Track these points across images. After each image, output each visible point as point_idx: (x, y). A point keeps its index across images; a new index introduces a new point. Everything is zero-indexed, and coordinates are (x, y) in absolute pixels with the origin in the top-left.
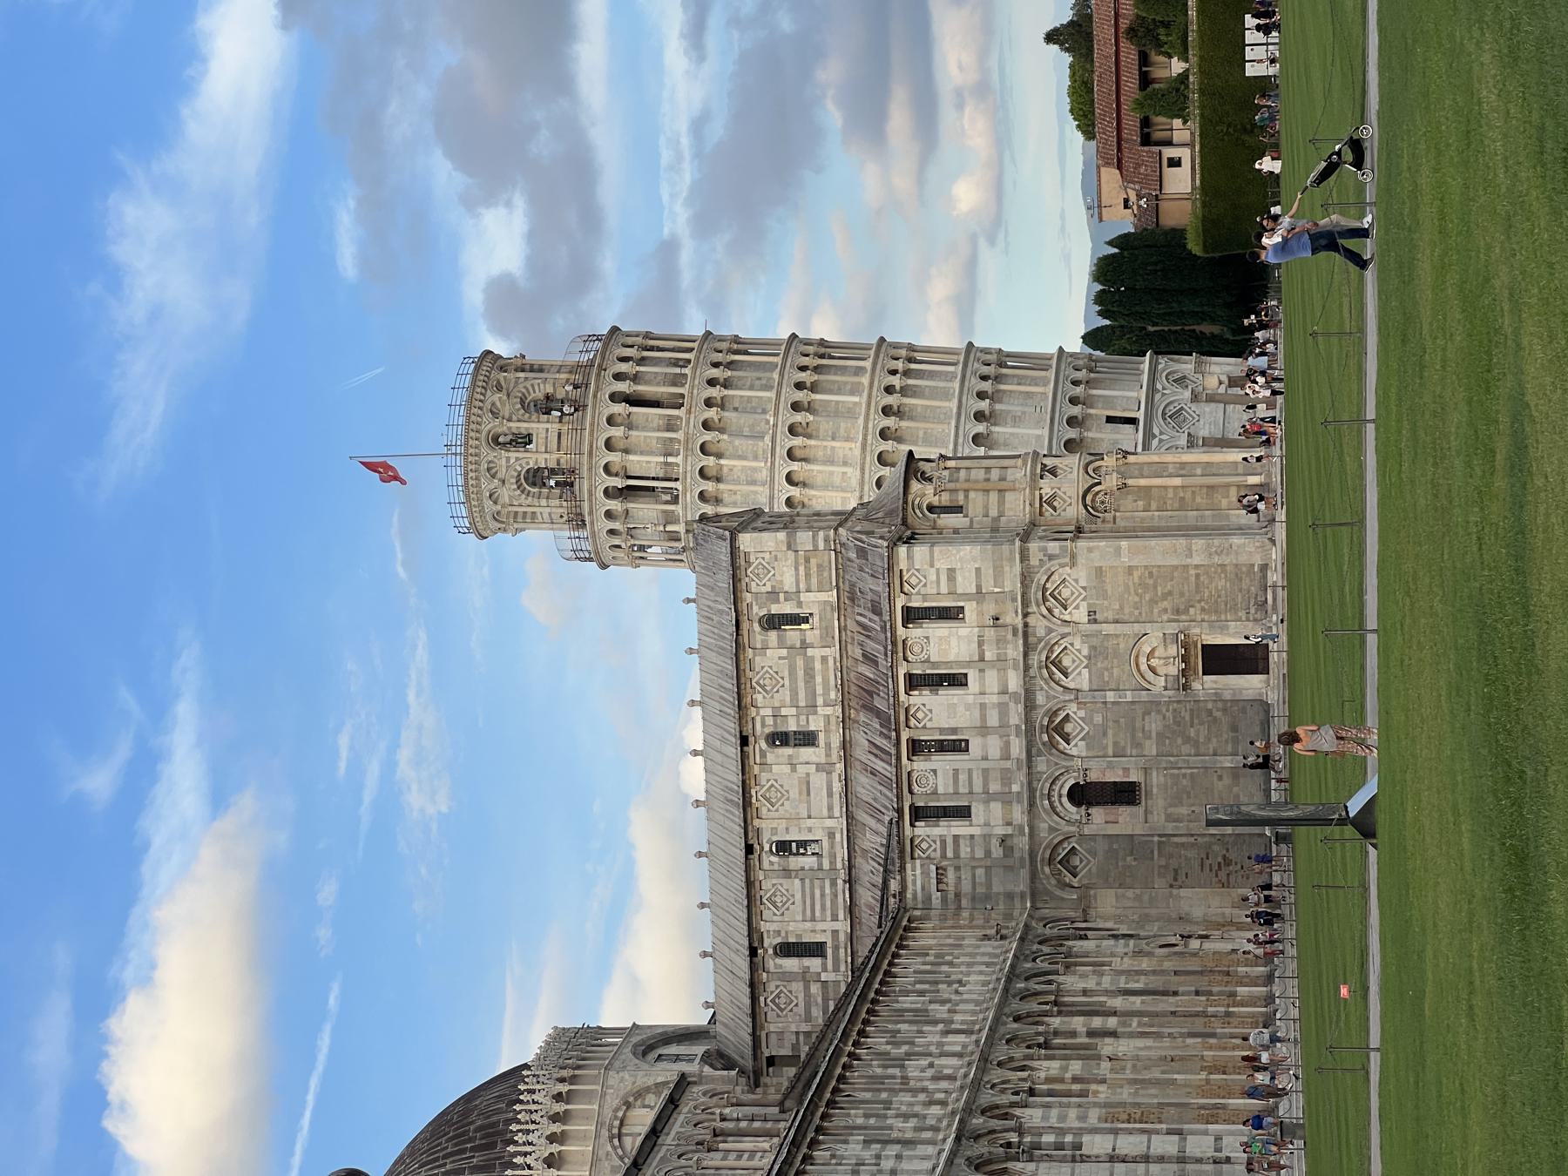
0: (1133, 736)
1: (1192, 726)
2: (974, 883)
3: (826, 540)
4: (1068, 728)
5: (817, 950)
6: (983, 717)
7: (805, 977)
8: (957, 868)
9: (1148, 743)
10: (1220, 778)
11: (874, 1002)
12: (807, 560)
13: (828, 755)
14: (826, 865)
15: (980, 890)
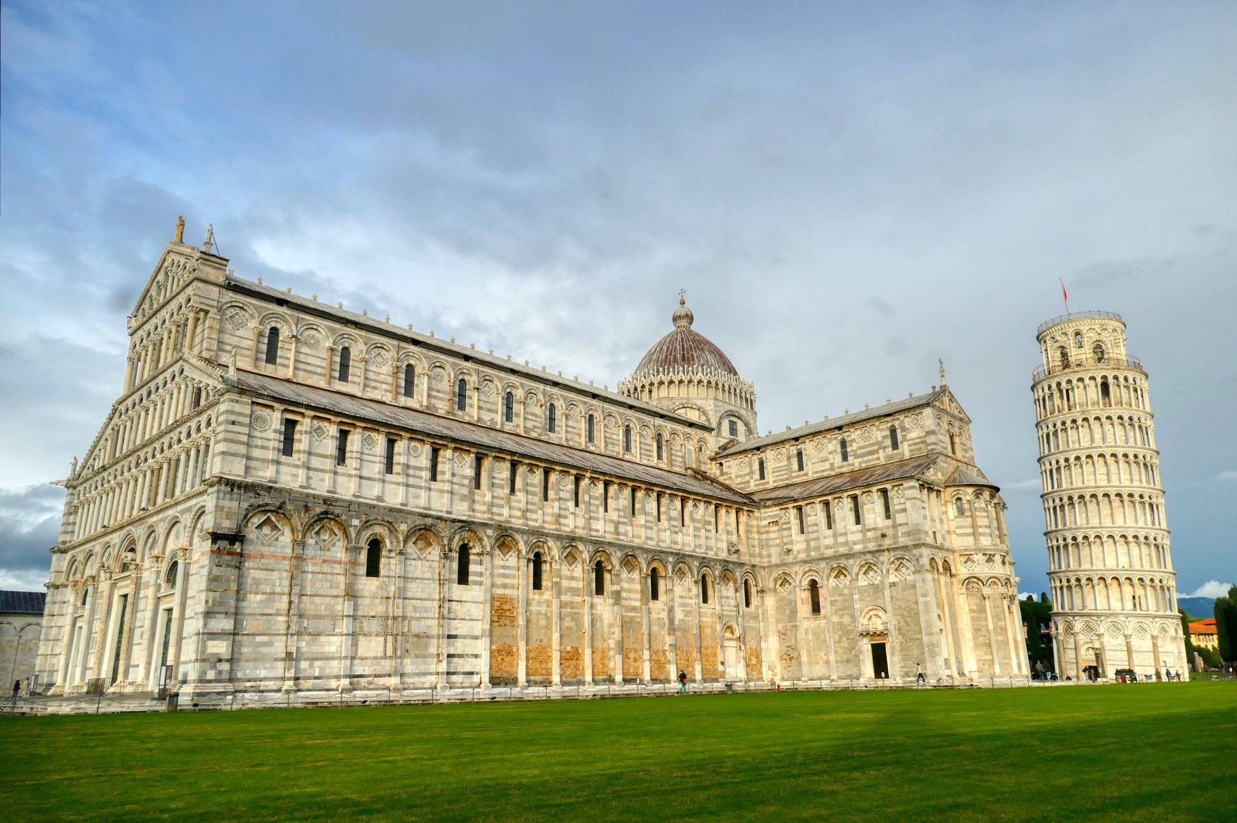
0: (840, 610)
1: (848, 639)
2: (773, 539)
3: (932, 450)
4: (842, 577)
5: (762, 477)
6: (842, 535)
7: (752, 472)
8: (778, 531)
9: (838, 617)
10: (826, 654)
11: (652, 490)
12: (922, 442)
13: (838, 468)
14: (793, 475)
15: (771, 543)
